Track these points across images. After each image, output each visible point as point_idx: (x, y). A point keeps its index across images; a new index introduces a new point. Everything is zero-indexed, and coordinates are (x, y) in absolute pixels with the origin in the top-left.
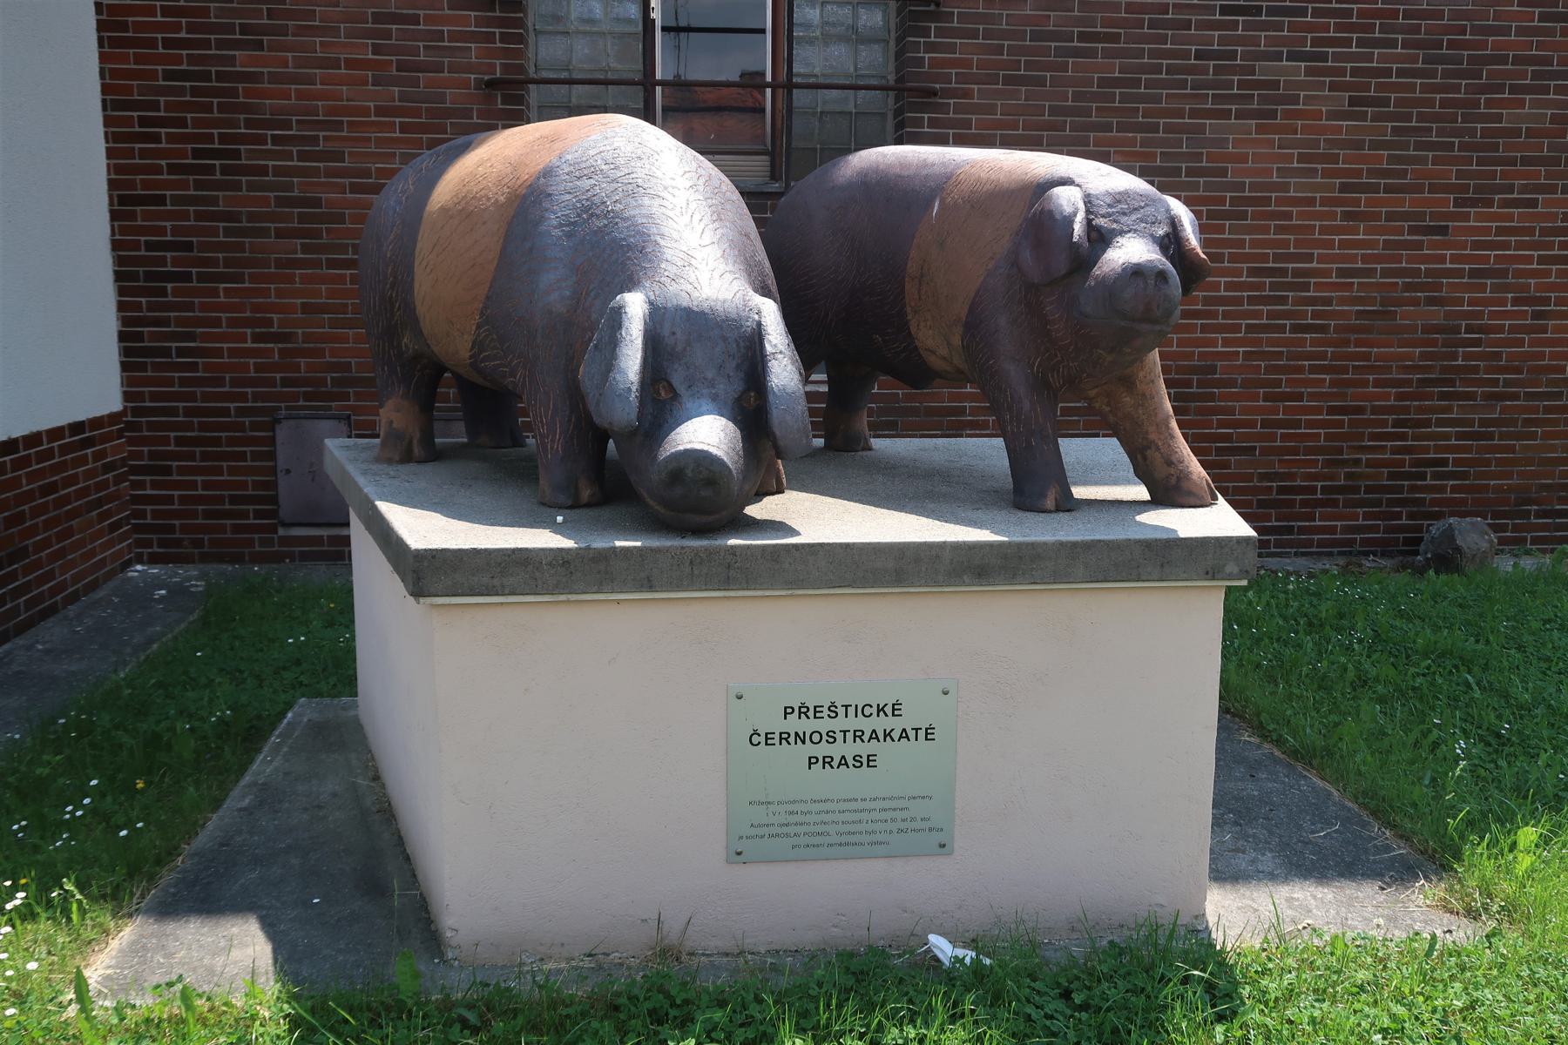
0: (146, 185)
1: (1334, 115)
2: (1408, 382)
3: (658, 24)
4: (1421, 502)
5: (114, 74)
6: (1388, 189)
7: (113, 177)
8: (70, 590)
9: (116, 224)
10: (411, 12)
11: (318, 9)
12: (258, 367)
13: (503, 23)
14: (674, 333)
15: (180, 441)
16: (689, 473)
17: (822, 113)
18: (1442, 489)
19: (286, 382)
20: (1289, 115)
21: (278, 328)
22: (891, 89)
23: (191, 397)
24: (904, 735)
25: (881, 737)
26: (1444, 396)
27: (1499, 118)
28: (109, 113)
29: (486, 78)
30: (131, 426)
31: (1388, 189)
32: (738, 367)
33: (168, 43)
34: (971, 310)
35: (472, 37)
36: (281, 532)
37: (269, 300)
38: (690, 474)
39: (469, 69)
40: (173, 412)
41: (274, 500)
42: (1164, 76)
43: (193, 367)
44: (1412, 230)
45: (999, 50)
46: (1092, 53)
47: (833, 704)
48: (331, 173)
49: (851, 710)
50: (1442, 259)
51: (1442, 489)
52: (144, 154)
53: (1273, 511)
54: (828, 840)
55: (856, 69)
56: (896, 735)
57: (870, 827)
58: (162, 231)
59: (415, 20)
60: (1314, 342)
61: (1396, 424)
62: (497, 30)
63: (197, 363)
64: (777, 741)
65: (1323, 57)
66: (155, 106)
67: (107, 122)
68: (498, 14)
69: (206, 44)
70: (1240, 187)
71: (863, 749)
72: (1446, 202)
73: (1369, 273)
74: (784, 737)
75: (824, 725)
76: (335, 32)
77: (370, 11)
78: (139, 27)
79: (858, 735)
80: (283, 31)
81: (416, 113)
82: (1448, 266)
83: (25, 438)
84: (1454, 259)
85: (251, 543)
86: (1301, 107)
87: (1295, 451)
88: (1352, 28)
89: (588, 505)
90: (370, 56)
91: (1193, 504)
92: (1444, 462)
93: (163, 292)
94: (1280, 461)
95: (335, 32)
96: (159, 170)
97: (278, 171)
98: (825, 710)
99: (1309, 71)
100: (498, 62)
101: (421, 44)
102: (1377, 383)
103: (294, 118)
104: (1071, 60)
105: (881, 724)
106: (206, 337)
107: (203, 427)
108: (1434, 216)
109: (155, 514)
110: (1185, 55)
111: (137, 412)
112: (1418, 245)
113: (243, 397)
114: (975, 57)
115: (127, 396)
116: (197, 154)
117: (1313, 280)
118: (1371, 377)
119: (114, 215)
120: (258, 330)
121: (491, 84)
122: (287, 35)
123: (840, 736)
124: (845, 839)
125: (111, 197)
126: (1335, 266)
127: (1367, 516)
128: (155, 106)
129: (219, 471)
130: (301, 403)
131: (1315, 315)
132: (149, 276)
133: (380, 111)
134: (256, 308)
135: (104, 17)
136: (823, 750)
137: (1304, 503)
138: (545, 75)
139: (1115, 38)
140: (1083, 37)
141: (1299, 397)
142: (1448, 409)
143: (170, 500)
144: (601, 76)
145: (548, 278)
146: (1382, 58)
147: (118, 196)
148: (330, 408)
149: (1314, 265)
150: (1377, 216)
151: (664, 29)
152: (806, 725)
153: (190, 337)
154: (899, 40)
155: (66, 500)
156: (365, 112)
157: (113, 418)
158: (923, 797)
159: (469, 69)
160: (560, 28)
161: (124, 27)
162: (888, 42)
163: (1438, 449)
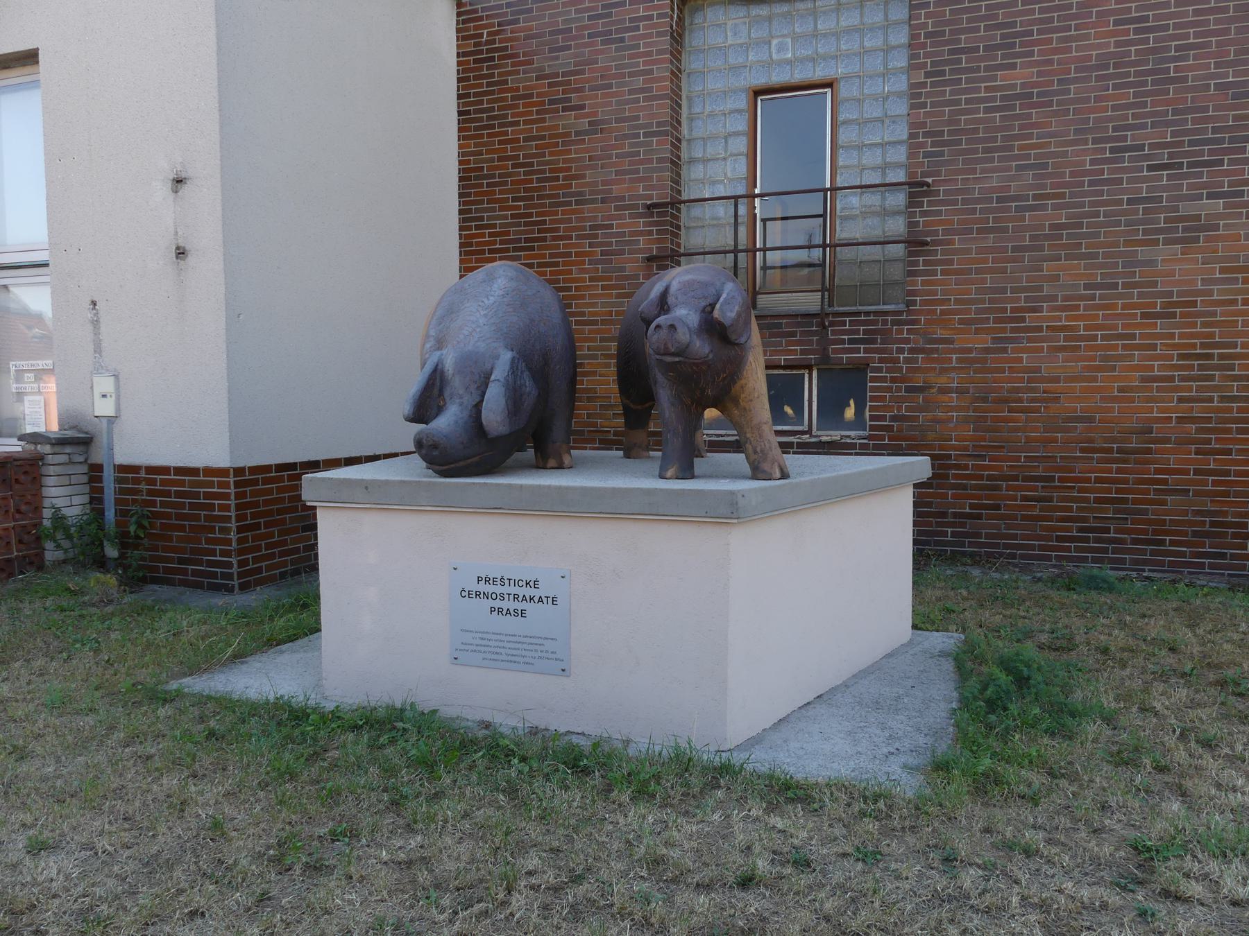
3: (758, 216)
17: (860, 262)
24: (540, 600)
25: (528, 600)
35: (641, 233)
42: (1101, 219)
46: (1044, 208)
47: (502, 578)
49: (512, 582)
53: (1207, 540)
54: (501, 657)
56: (536, 599)
57: (524, 653)
64: (474, 596)
70: (1171, 294)
71: (520, 606)
74: (478, 594)
75: (498, 589)
78: (478, 244)
79: (516, 597)
87: (1227, 494)
94: (1212, 501)
98: (498, 580)
105: (529, 592)
117: (1237, 362)
121: (650, 259)
123: (506, 597)
124: (510, 658)
136: (497, 604)
141: (1229, 452)
149: (1238, 350)
152: (489, 589)
158: (552, 639)
161: (471, 245)
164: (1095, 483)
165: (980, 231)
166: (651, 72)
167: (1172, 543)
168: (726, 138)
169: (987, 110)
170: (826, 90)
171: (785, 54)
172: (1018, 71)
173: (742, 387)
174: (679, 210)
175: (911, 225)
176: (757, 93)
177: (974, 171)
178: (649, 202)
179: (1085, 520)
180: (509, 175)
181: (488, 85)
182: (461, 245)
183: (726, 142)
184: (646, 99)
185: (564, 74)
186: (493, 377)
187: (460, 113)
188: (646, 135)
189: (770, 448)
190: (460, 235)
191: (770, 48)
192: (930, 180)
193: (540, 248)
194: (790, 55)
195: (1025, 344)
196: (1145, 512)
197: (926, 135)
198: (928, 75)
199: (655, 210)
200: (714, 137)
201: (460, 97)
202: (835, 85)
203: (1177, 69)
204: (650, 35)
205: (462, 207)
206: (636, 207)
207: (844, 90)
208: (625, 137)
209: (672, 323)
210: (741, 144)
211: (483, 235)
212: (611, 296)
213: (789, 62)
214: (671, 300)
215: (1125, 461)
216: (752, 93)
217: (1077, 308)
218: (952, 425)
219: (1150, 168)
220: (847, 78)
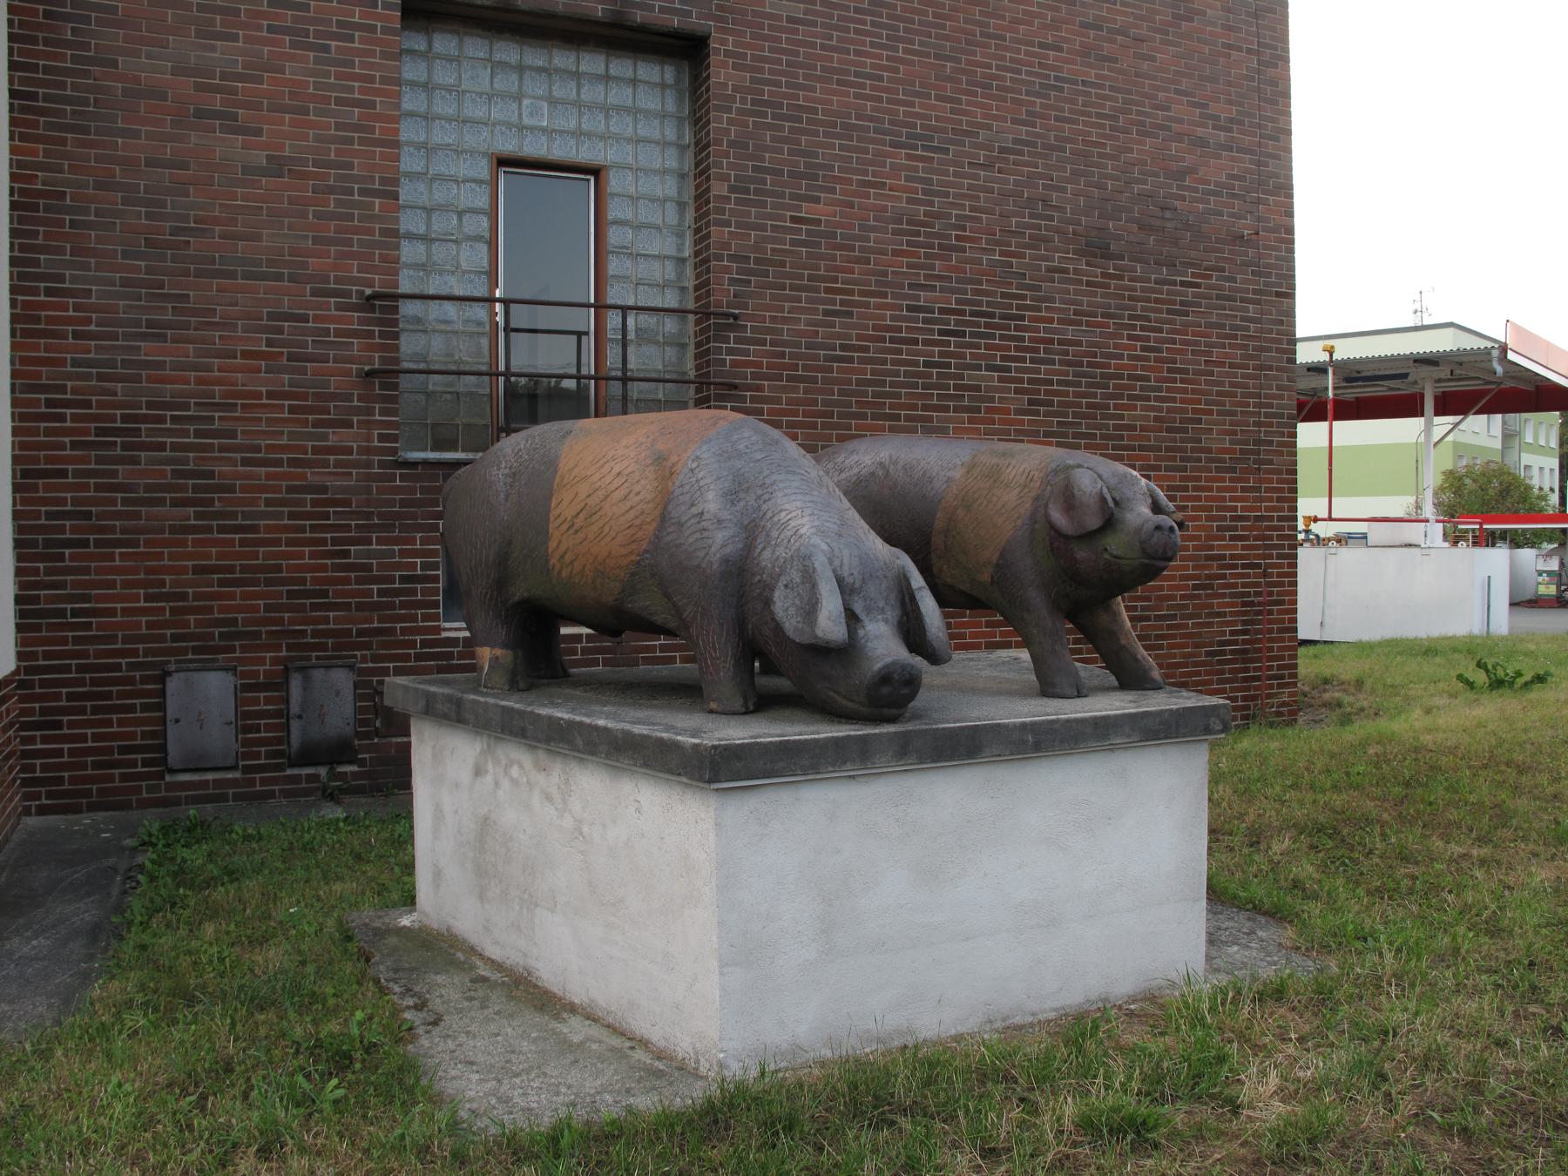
0: (49, 460)
1: (1019, 412)
7: (17, 452)
9: (18, 495)
10: (302, 312)
11: (218, 308)
12: (150, 625)
13: (380, 322)
14: (852, 574)
15: (70, 697)
16: (896, 677)
19: (175, 638)
20: (988, 410)
21: (170, 588)
22: (693, 382)
23: (85, 655)
27: (1122, 417)
28: (18, 395)
29: (367, 368)
30: (22, 684)
34: (1002, 555)
36: (168, 778)
37: (162, 563)
39: (351, 360)
40: (67, 669)
41: (163, 748)
43: (88, 626)
45: (782, 355)
46: (850, 360)
48: (223, 449)
52: (48, 432)
55: (664, 366)
58: (63, 501)
62: (376, 329)
63: (91, 623)
65: (1008, 370)
66: (63, 389)
67: (15, 403)
68: (377, 315)
77: (265, 310)
81: (304, 397)
85: (138, 790)
88: (1026, 349)
89: (752, 712)
90: (264, 348)
93: (61, 558)
96: (62, 447)
97: (175, 447)
99: (1001, 379)
100: (377, 355)
101: (310, 339)
103: (192, 401)
106: (100, 598)
107: (94, 682)
109: (44, 768)
110: (916, 364)
111: (28, 670)
113: (135, 653)
114: (765, 360)
115: (20, 656)
116: (100, 432)
119: (16, 488)
120: (151, 591)
121: (369, 374)
122: (189, 329)
125: (14, 471)
128: (63, 389)
129: (109, 723)
130: (190, 656)
132: (48, 543)
133: (270, 395)
134: (149, 570)
135: (18, 311)
140: (844, 347)
143: (60, 753)
144: (453, 367)
146: (1047, 372)
147: (21, 470)
148: (216, 660)
153: (85, 598)
154: (698, 345)
156: (258, 395)
159: (351, 360)
165: (790, 379)
168: (460, 214)
170: (588, 177)
171: (539, 120)
176: (503, 162)
178: (368, 291)
182: (14, 319)
184: (362, 141)
185: (224, 76)
190: (13, 303)
191: (520, 108)
198: (732, 189)
200: (444, 208)
202: (603, 174)
204: (372, 54)
206: (348, 294)
207: (614, 182)
208: (331, 190)
212: (305, 423)
213: (544, 130)
216: (495, 160)
219: (941, 333)
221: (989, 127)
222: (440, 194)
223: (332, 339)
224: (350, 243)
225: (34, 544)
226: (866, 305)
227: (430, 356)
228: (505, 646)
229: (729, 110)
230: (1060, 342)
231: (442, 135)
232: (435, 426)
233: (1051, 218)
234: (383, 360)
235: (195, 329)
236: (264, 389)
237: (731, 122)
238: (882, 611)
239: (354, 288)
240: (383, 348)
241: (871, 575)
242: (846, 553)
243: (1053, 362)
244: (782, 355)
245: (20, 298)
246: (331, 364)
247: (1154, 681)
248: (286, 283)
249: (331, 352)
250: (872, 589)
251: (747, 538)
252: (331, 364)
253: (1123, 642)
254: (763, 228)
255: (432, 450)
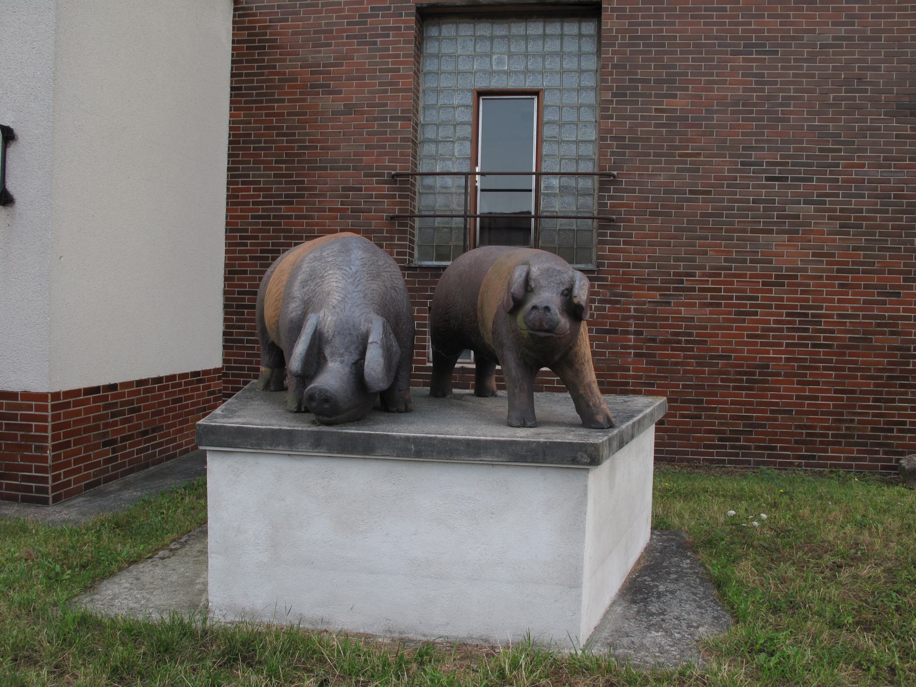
0: (240, 265)
2: (881, 378)
3: (479, 188)
4: (891, 445)
5: (232, 217)
6: (864, 272)
8: (184, 448)
16: (316, 395)
17: (559, 230)
18: (903, 438)
20: (805, 232)
26: (902, 386)
28: (228, 234)
29: (391, 215)
30: (225, 375)
31: (864, 272)
32: (356, 348)
33: (254, 203)
38: (317, 397)
39: (383, 211)
40: (243, 369)
44: (879, 294)
45: (647, 199)
46: (697, 200)
50: (898, 310)
51: (903, 438)
52: (240, 252)
55: (577, 208)
58: (244, 286)
59: (360, 190)
60: (825, 354)
61: (875, 400)
67: (227, 238)
68: (398, 186)
69: (269, 203)
70: (781, 269)
72: (898, 280)
73: (857, 317)
76: (325, 196)
78: (244, 197)
80: (302, 196)
82: (901, 314)
83: (166, 377)
84: (905, 310)
86: (812, 228)
87: (816, 413)
88: (839, 188)
90: (340, 206)
91: (598, 427)
92: (904, 423)
93: (243, 314)
95: (325, 196)
96: (245, 259)
100: (397, 208)
101: (362, 200)
102: (863, 377)
104: (685, 204)
108: (892, 287)
110: (747, 201)
111: (228, 368)
112: (884, 303)
114: (634, 202)
115: (225, 361)
116: (262, 251)
117: (823, 320)
118: (859, 374)
119: (226, 279)
121: (392, 218)
125: (225, 271)
126: (835, 312)
127: (859, 452)
128: (246, 231)
131: (825, 339)
132: (238, 306)
137: (822, 443)
138: (423, 213)
139: (709, 193)
140: (691, 192)
141: (817, 383)
142: (906, 393)
144: (449, 213)
145: (293, 306)
149: (824, 311)
150: (859, 286)
151: (482, 190)
155: (187, 406)
157: (216, 371)
159: (383, 211)
160: (431, 191)
161: (237, 197)
162: (594, 195)
163: (900, 416)
164: (731, 405)
165: (651, 214)
166: (398, 70)
167: (782, 449)
168: (455, 126)
169: (657, 126)
170: (533, 97)
171: (503, 67)
172: (678, 100)
173: (576, 353)
174: (415, 180)
175: (600, 205)
176: (480, 93)
177: (647, 169)
178: (393, 172)
179: (724, 432)
180: (274, 142)
181: (259, 67)
182: (228, 197)
183: (455, 129)
184: (392, 91)
185: (325, 66)
186: (370, 340)
187: (232, 89)
188: (392, 119)
189: (600, 402)
190: (228, 189)
191: (491, 61)
192: (615, 173)
193: (298, 203)
194: (506, 68)
195: (683, 300)
196: (764, 426)
197: (612, 139)
198: (614, 95)
199: (398, 179)
200: (443, 124)
201: (233, 75)
203: (783, 112)
204: (399, 42)
205: (230, 166)
206: (382, 175)
207: (548, 99)
209: (547, 305)
210: (467, 131)
211: (248, 190)
213: (505, 72)
214: (533, 284)
215: (752, 389)
216: (476, 93)
217: (719, 275)
218: (630, 360)
219: (767, 179)
220: (550, 89)
221: (813, 31)
222: (444, 116)
223: (374, 200)
224: (384, 147)
225: (232, 306)
226: (710, 163)
227: (437, 208)
228: (267, 366)
229: (613, 45)
230: (870, 181)
231: (444, 82)
232: (438, 246)
233: (866, 91)
234: (400, 210)
235: (307, 198)
236: (339, 228)
237: (614, 52)
238: (342, 355)
239: (386, 172)
240: (401, 203)
241: (339, 333)
242: (329, 319)
243: (863, 196)
244: (647, 199)
245: (231, 187)
246: (373, 214)
247: (597, 422)
248: (351, 171)
249: (373, 207)
250: (337, 341)
251: (304, 308)
252: (373, 214)
253: (581, 392)
254: (636, 118)
255: (436, 261)
